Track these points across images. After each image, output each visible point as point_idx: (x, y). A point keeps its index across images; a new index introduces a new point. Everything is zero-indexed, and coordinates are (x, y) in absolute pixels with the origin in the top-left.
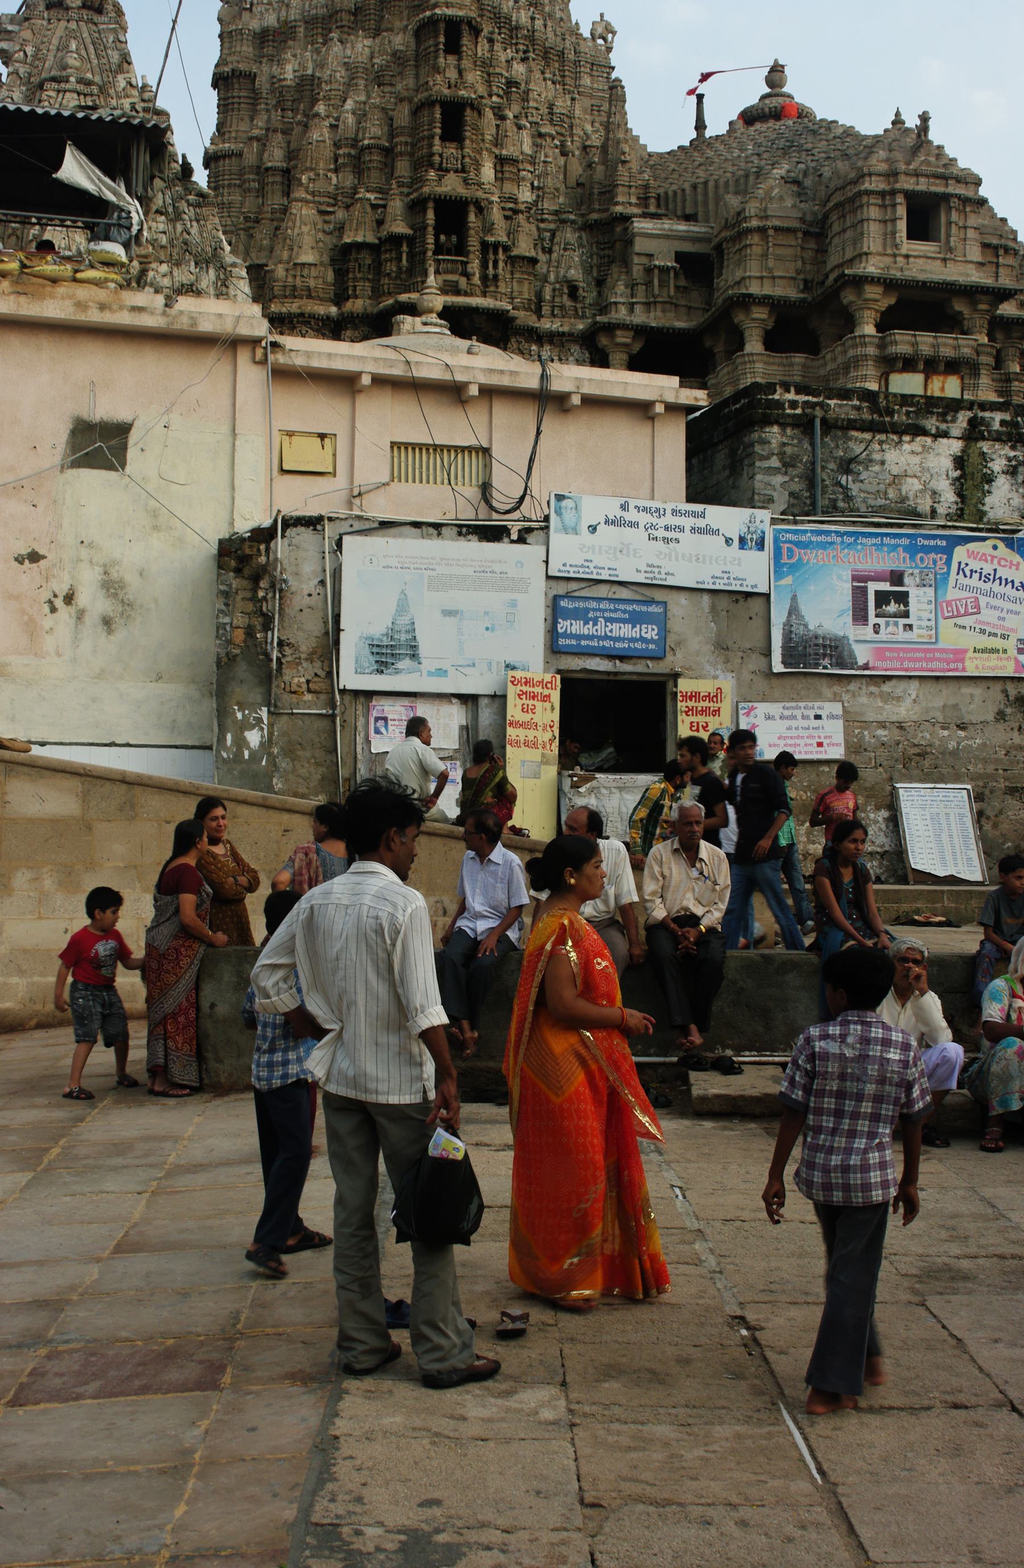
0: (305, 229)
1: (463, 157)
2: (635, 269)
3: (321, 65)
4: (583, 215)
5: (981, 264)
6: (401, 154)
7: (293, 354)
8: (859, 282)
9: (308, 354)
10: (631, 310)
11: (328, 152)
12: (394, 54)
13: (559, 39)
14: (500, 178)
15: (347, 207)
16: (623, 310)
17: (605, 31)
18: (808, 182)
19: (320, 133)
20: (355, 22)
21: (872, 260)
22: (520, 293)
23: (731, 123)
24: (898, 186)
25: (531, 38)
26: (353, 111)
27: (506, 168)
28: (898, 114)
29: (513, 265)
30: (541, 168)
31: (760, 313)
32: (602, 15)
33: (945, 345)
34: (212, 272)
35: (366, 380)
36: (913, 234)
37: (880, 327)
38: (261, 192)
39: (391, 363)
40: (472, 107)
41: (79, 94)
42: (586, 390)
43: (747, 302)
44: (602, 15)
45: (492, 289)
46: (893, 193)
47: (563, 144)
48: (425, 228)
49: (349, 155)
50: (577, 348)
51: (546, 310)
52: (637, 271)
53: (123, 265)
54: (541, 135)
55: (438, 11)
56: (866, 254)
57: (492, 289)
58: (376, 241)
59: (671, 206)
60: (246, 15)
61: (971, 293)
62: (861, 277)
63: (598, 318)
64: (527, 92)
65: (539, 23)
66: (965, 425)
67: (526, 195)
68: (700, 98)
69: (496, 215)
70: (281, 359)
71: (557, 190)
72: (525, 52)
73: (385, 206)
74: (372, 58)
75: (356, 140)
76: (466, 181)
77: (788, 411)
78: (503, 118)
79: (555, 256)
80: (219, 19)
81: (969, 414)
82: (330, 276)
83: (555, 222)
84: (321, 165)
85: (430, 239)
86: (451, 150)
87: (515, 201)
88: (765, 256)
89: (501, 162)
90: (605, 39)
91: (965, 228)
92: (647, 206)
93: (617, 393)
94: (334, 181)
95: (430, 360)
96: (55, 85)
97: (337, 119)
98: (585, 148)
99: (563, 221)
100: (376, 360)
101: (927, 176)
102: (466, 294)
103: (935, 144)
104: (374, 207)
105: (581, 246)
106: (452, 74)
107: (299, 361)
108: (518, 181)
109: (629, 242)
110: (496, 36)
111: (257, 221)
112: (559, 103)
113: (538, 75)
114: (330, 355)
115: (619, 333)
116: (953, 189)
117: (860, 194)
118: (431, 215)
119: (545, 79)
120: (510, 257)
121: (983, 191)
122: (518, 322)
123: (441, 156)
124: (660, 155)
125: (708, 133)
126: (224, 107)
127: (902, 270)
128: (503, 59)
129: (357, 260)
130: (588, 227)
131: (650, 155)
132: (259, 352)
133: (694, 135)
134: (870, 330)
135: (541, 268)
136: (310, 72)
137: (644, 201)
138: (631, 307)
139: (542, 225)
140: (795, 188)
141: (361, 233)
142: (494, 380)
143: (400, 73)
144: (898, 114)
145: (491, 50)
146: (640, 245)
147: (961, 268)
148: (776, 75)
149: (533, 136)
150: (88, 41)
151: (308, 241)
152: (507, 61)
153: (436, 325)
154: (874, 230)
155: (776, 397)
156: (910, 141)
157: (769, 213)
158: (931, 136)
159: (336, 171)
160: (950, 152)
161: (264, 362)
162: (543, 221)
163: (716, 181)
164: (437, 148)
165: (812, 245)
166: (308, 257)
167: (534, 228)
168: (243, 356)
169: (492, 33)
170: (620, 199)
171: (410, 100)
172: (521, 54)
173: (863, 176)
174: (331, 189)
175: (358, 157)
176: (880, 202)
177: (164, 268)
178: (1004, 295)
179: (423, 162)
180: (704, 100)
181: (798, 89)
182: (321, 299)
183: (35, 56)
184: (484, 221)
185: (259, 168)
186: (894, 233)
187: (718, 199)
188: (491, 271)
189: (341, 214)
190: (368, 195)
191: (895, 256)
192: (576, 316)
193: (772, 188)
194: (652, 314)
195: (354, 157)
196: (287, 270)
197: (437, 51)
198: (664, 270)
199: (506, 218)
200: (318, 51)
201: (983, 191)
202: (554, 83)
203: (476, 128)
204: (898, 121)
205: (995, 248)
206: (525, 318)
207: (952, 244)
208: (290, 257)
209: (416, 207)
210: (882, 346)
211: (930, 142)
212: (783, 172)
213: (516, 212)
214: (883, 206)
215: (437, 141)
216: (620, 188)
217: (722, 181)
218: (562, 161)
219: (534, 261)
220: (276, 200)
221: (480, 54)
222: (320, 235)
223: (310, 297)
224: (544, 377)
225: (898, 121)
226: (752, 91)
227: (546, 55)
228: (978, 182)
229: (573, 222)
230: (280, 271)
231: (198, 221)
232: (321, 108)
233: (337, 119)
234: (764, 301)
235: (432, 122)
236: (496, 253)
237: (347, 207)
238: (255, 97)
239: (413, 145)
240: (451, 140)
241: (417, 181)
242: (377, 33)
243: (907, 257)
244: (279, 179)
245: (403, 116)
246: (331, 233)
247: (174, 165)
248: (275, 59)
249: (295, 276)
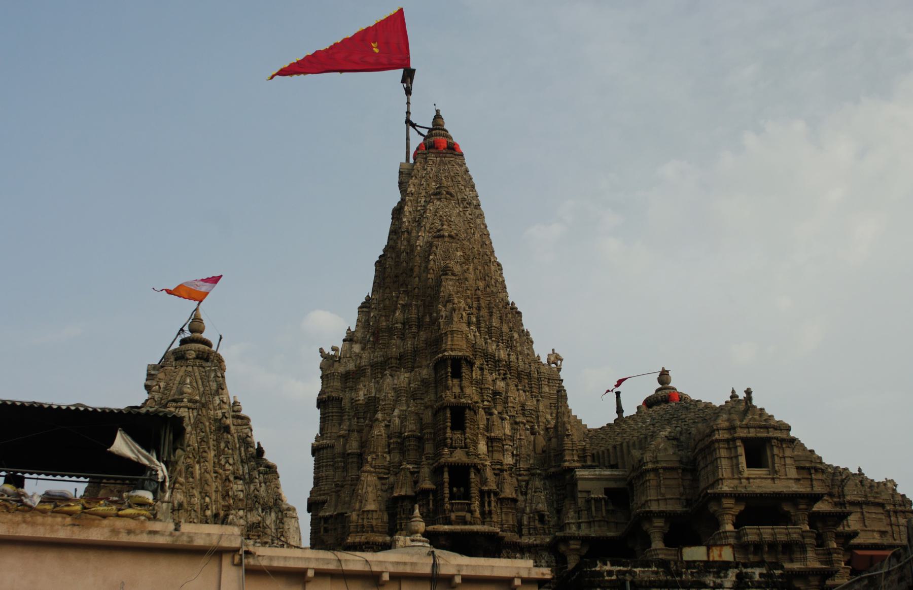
0: (370, 489)
1: (465, 439)
2: (579, 501)
3: (379, 390)
4: (545, 470)
5: (797, 480)
6: (428, 440)
7: (260, 558)
8: (719, 497)
9: (271, 558)
10: (579, 527)
11: (384, 442)
12: (423, 381)
13: (527, 366)
14: (491, 450)
15: (396, 474)
16: (574, 528)
17: (555, 359)
18: (683, 438)
19: (379, 431)
20: (400, 364)
21: (726, 483)
22: (507, 521)
23: (638, 408)
24: (736, 435)
25: (508, 366)
26: (398, 416)
27: (495, 444)
28: (733, 392)
29: (501, 504)
30: (517, 443)
31: (659, 523)
32: (553, 350)
33: (780, 533)
34: (273, 514)
35: (310, 573)
37: (736, 525)
38: (345, 469)
39: (328, 561)
40: (470, 409)
41: (189, 409)
42: (464, 573)
43: (649, 516)
44: (553, 350)
45: (488, 519)
46: (734, 440)
47: (532, 428)
48: (443, 484)
49: (397, 443)
50: (547, 554)
51: (525, 531)
52: (581, 502)
53: (150, 505)
54: (516, 423)
55: (446, 354)
56: (722, 479)
57: (488, 519)
58: (413, 494)
59: (601, 460)
60: (336, 364)
61: (793, 498)
62: (719, 494)
63: (557, 534)
64: (507, 398)
65: (513, 357)
66: (734, 579)
67: (509, 460)
68: (618, 394)
69: (489, 473)
70: (252, 561)
71: (529, 455)
72: (505, 374)
73: (418, 472)
74: (410, 383)
75: (401, 433)
76: (467, 454)
77: (607, 578)
78: (491, 414)
79: (529, 496)
80: (321, 368)
81: (736, 571)
82: (386, 517)
83: (528, 475)
84: (380, 449)
85: (447, 491)
86: (458, 435)
87: (501, 464)
88: (659, 486)
89: (491, 441)
90: (556, 364)
91: (784, 457)
92: (585, 461)
93: (487, 573)
94: (388, 459)
95: (357, 558)
96: (174, 404)
97: (389, 421)
98: (547, 429)
99: (533, 475)
100: (317, 559)
101: (755, 428)
102: (471, 524)
103: (759, 407)
104: (412, 473)
105: (545, 489)
106: (457, 390)
107: (264, 563)
108: (503, 451)
109: (575, 485)
110: (485, 366)
111: (342, 486)
112: (529, 403)
113: (513, 387)
114: (285, 558)
115: (572, 542)
116: (773, 434)
117: (713, 442)
118: (446, 475)
119: (518, 390)
120: (499, 499)
121: (793, 434)
122: (506, 539)
123: (451, 439)
124: (596, 430)
125: (625, 415)
126: (324, 419)
127: (745, 487)
129: (402, 506)
130: (548, 477)
131: (589, 431)
132: (237, 558)
133: (616, 416)
134: (729, 527)
135: (520, 504)
136: (373, 395)
137: (583, 458)
138: (579, 526)
139: (520, 478)
140: (675, 443)
141: (404, 490)
142: (400, 569)
143: (426, 392)
144: (733, 392)
145: (482, 375)
146: (581, 486)
147: (785, 483)
148: (664, 377)
149: (511, 424)
150: (198, 377)
151: (371, 497)
152: (493, 381)
153: (420, 541)
154: (725, 463)
155: (598, 569)
156: (742, 407)
157: (659, 459)
158: (754, 403)
159: (389, 453)
160: (769, 411)
161: (240, 564)
162: (520, 475)
163: (628, 443)
164: (449, 434)
165: (689, 477)
166: (371, 506)
167: (514, 480)
168: (226, 560)
169: (482, 364)
170: (567, 458)
171: (432, 407)
172: (502, 376)
173: (714, 431)
174: (386, 464)
175: (402, 444)
176: (726, 446)
177: (241, 513)
178: (817, 498)
179: (441, 443)
180: (621, 395)
181: (678, 384)
182: (381, 532)
183: (165, 388)
184: (481, 478)
185: (344, 454)
186: (738, 464)
187: (629, 452)
188: (487, 508)
189: (392, 479)
190: (408, 466)
191: (740, 479)
192: (545, 533)
193: (660, 444)
194: (592, 529)
195: (400, 443)
196: (358, 515)
197: (447, 377)
198: (597, 500)
199: (495, 474)
200: (378, 382)
201: (793, 434)
202: (524, 391)
203: (473, 421)
204: (734, 396)
205: (809, 469)
206: (510, 537)
207: (777, 468)
208: (360, 508)
209: (437, 472)
210: (738, 537)
211: (755, 407)
212: (667, 433)
213: (502, 470)
214: (729, 449)
215: (449, 430)
216: (567, 452)
217: (631, 442)
218: (532, 437)
219: (515, 501)
220: (353, 473)
221: (474, 377)
222: (379, 493)
223: (373, 531)
224: (435, 565)
225: (734, 396)
226: (651, 387)
227: (519, 376)
228: (788, 428)
229: (539, 475)
230: (354, 516)
231: (265, 483)
232: (379, 416)
233: (389, 421)
234: (660, 514)
235: (445, 419)
236: (489, 497)
237: (396, 474)
238: (342, 411)
239: (435, 434)
240: (457, 429)
241: (438, 455)
242: (412, 370)
243: (748, 479)
244: (355, 460)
245: (428, 416)
246: (386, 491)
247: (251, 449)
248: (354, 389)
249: (363, 519)
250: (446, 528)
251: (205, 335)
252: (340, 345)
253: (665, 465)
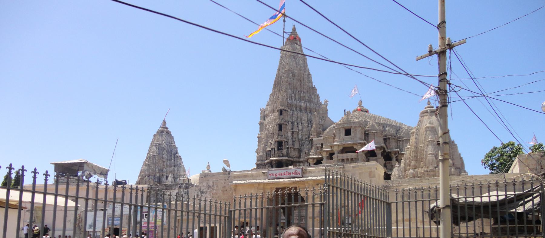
69: (290, 142)
82: (265, 155)
89: (293, 133)
128: (296, 113)
251: (167, 126)
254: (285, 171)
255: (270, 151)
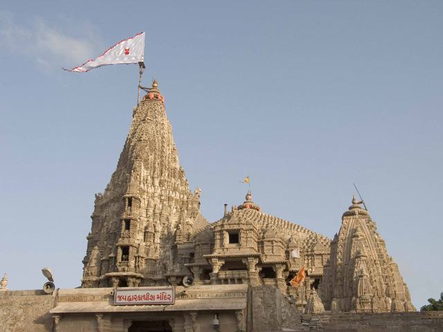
36: (231, 242)
86: (127, 231)
146: (179, 252)
205: (272, 241)
250: (114, 274)
252: (103, 192)
253: (203, 242)
254: (144, 293)
255: (108, 260)
